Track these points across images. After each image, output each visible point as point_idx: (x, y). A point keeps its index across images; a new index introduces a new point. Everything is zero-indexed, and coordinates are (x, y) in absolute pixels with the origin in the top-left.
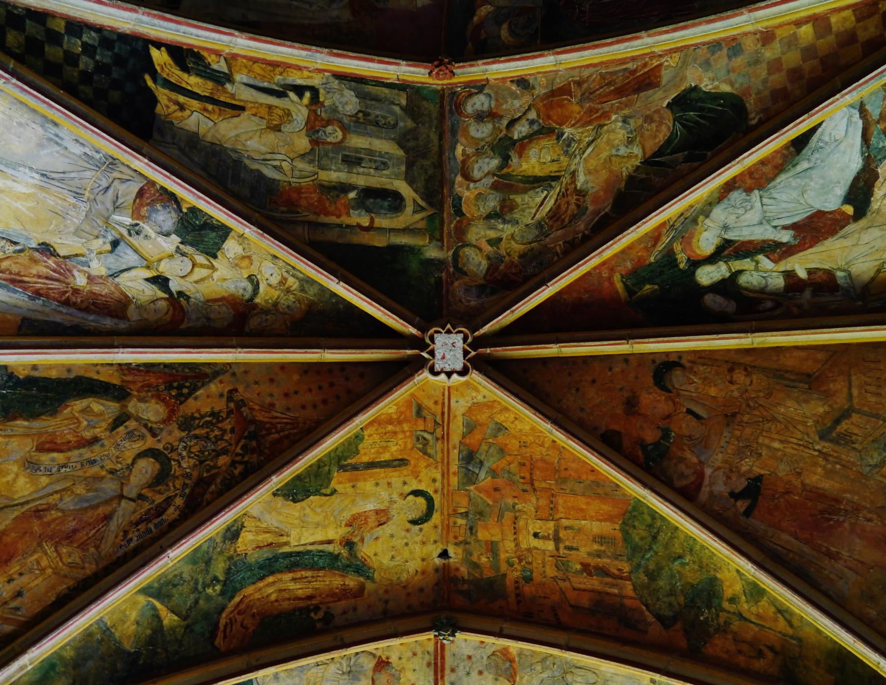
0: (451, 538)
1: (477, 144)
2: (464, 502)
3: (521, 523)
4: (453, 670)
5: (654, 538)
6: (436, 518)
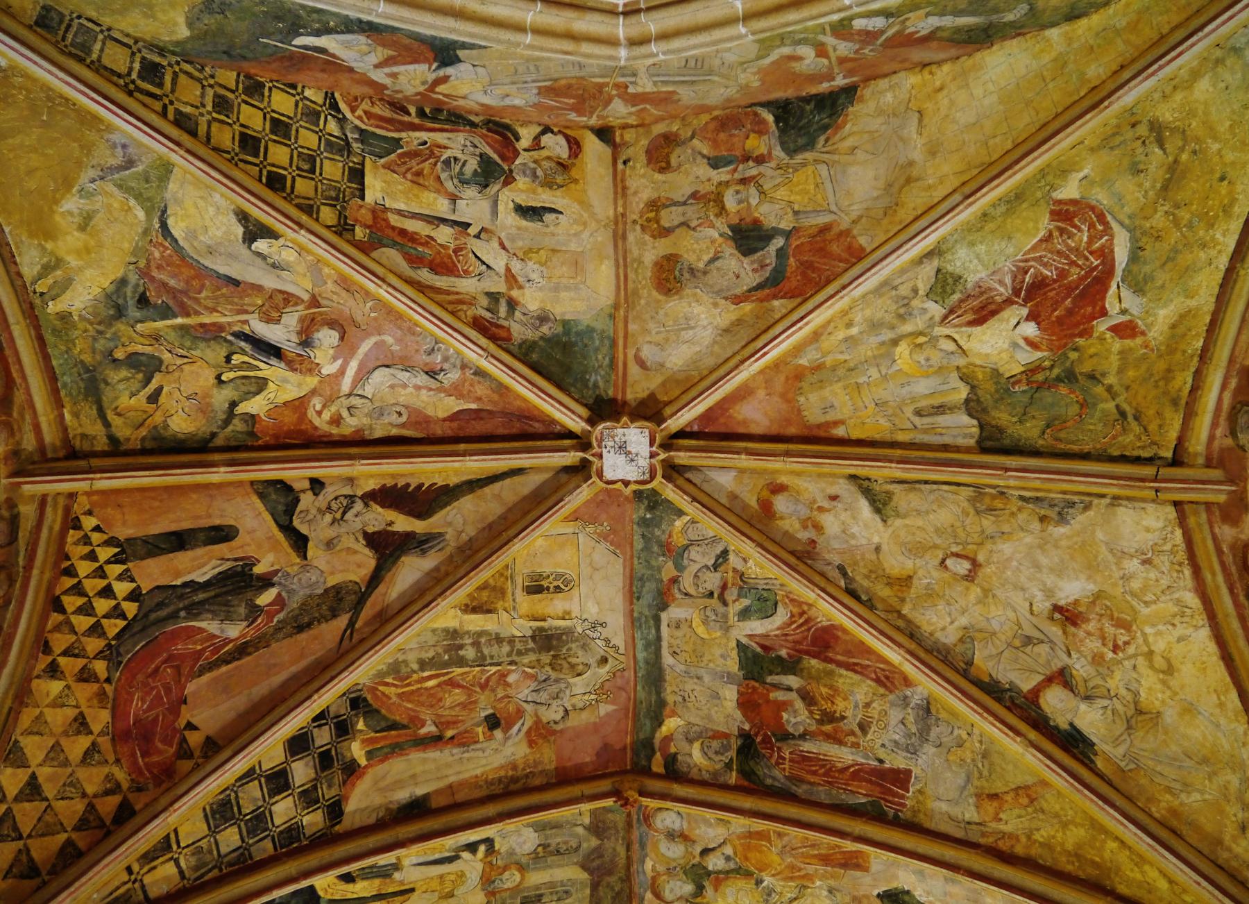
1: (668, 863)
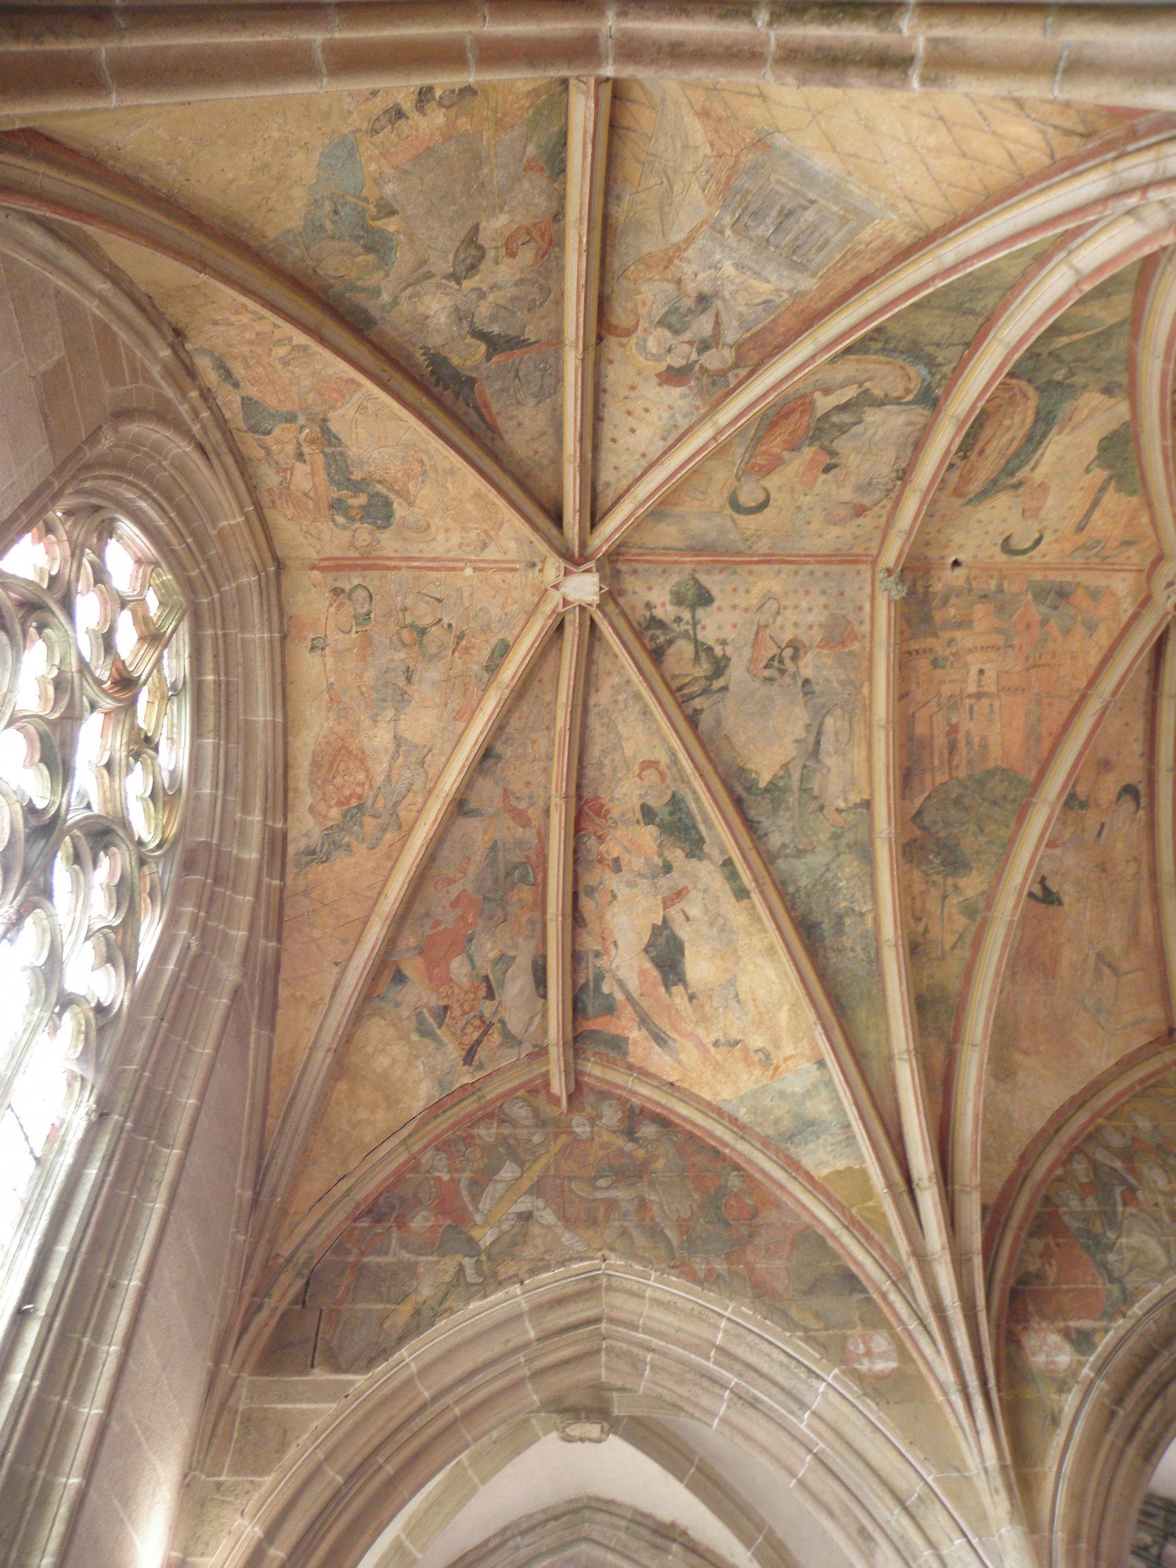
0: (973, 574)
2: (1014, 589)
3: (993, 655)
4: (826, 574)
5: (995, 803)
6: (1005, 557)
